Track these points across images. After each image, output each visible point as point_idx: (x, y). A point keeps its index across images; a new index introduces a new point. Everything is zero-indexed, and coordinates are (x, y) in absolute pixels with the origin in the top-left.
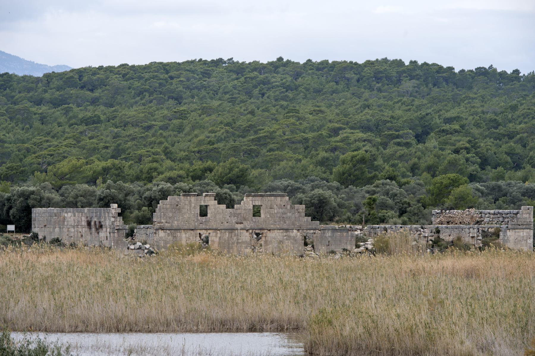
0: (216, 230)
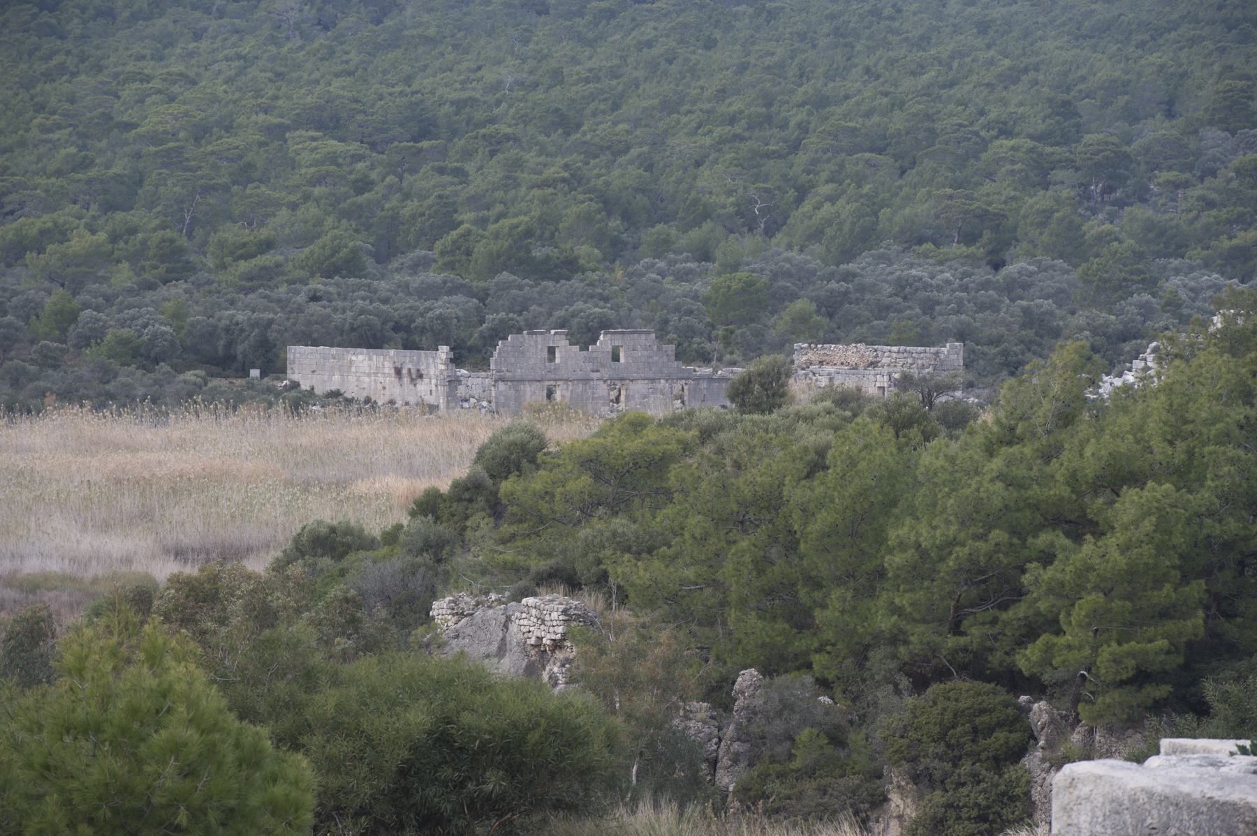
0: (567, 380)
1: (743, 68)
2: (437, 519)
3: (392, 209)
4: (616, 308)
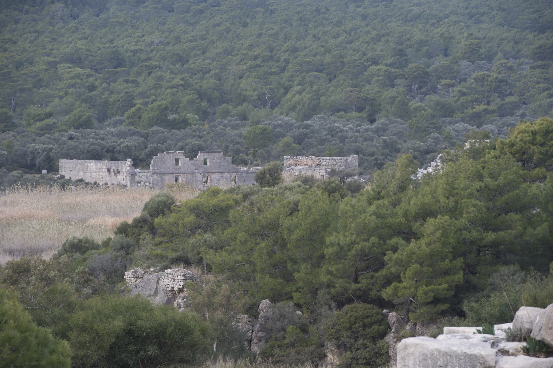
0: (184, 173)
1: (260, 35)
2: (127, 235)
3: (105, 98)
4: (205, 141)
